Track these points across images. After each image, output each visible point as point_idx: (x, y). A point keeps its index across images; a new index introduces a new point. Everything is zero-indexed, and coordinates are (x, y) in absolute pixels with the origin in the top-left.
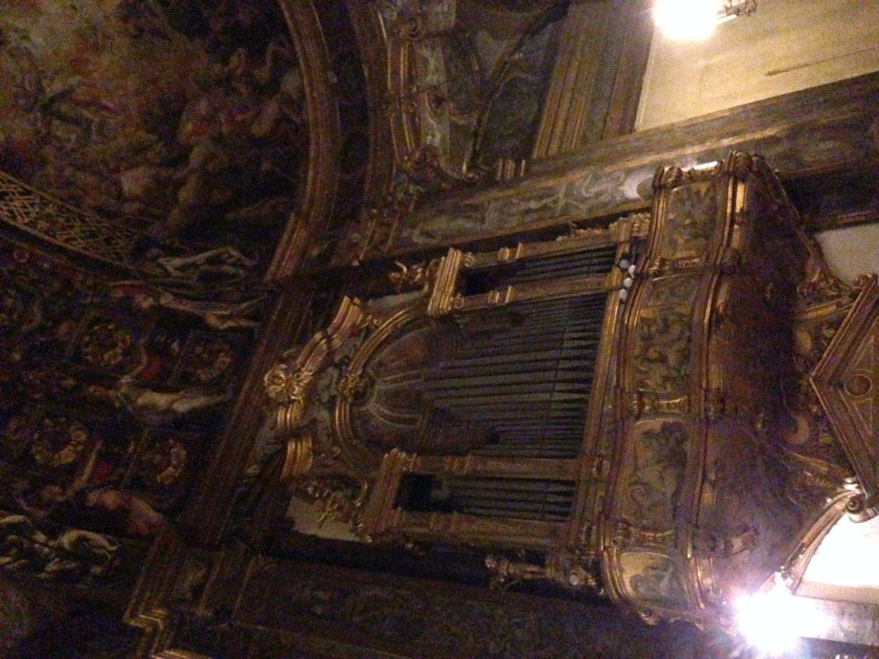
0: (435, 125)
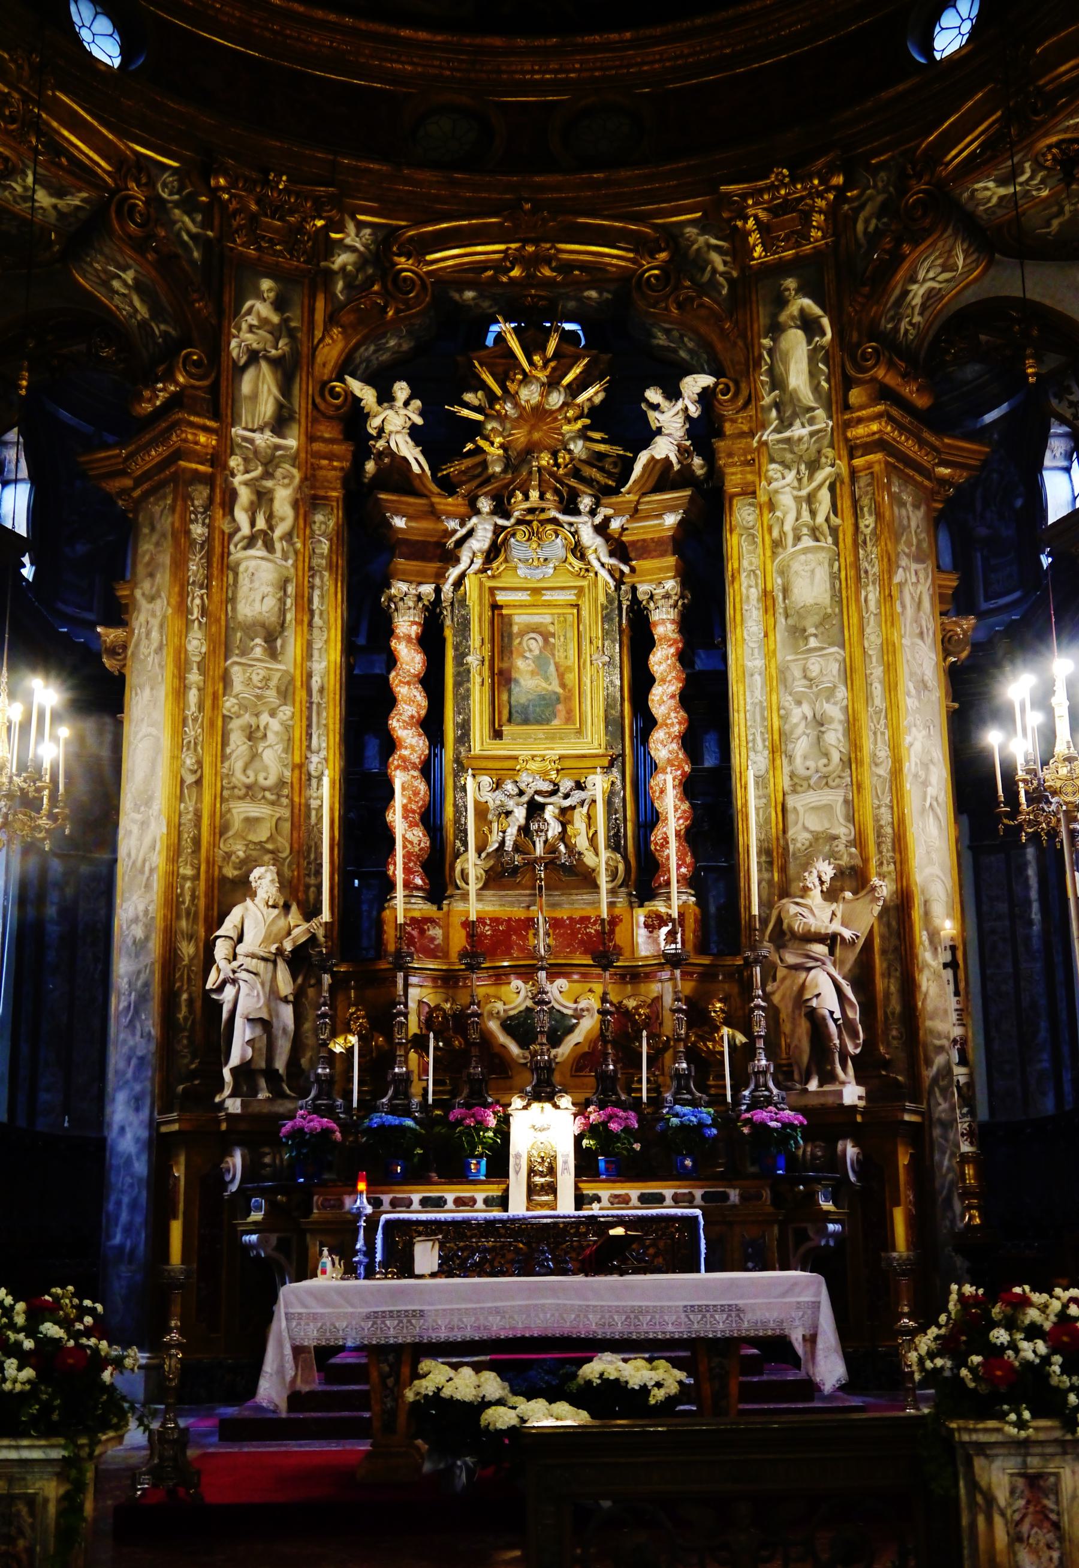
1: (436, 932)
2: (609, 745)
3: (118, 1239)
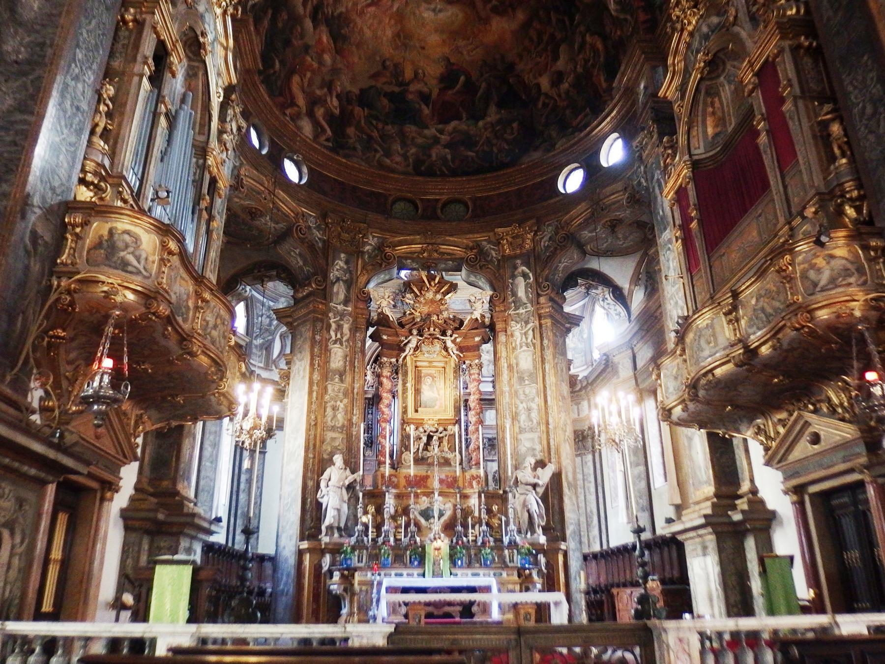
0: (242, 202)
1: (394, 479)
2: (455, 416)
3: (281, 587)
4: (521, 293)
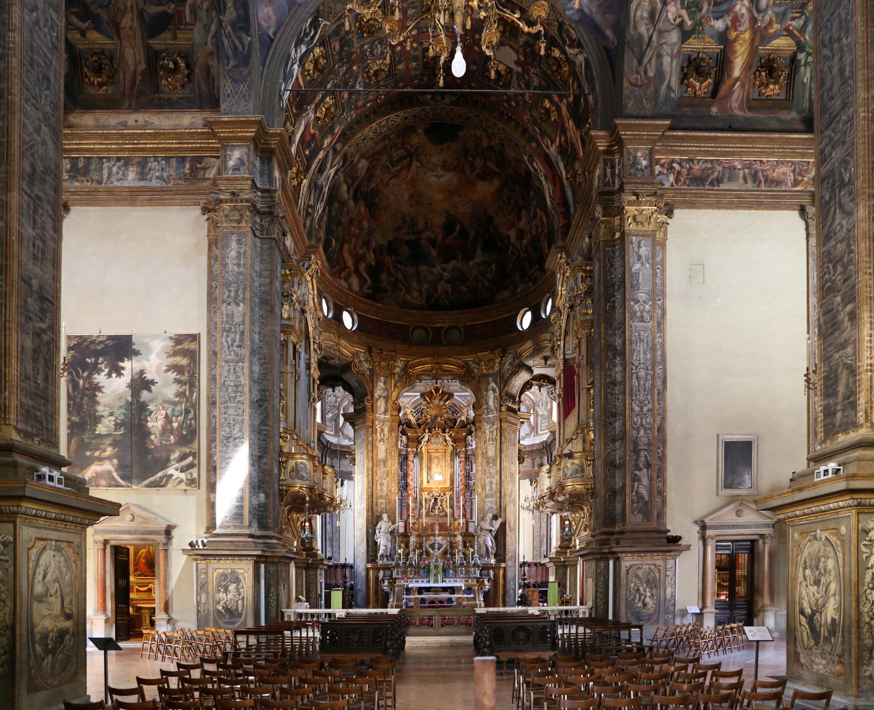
4: (491, 403)
